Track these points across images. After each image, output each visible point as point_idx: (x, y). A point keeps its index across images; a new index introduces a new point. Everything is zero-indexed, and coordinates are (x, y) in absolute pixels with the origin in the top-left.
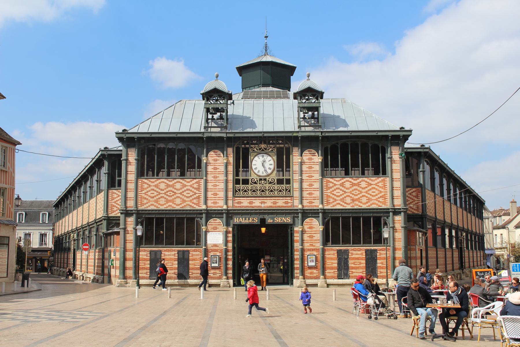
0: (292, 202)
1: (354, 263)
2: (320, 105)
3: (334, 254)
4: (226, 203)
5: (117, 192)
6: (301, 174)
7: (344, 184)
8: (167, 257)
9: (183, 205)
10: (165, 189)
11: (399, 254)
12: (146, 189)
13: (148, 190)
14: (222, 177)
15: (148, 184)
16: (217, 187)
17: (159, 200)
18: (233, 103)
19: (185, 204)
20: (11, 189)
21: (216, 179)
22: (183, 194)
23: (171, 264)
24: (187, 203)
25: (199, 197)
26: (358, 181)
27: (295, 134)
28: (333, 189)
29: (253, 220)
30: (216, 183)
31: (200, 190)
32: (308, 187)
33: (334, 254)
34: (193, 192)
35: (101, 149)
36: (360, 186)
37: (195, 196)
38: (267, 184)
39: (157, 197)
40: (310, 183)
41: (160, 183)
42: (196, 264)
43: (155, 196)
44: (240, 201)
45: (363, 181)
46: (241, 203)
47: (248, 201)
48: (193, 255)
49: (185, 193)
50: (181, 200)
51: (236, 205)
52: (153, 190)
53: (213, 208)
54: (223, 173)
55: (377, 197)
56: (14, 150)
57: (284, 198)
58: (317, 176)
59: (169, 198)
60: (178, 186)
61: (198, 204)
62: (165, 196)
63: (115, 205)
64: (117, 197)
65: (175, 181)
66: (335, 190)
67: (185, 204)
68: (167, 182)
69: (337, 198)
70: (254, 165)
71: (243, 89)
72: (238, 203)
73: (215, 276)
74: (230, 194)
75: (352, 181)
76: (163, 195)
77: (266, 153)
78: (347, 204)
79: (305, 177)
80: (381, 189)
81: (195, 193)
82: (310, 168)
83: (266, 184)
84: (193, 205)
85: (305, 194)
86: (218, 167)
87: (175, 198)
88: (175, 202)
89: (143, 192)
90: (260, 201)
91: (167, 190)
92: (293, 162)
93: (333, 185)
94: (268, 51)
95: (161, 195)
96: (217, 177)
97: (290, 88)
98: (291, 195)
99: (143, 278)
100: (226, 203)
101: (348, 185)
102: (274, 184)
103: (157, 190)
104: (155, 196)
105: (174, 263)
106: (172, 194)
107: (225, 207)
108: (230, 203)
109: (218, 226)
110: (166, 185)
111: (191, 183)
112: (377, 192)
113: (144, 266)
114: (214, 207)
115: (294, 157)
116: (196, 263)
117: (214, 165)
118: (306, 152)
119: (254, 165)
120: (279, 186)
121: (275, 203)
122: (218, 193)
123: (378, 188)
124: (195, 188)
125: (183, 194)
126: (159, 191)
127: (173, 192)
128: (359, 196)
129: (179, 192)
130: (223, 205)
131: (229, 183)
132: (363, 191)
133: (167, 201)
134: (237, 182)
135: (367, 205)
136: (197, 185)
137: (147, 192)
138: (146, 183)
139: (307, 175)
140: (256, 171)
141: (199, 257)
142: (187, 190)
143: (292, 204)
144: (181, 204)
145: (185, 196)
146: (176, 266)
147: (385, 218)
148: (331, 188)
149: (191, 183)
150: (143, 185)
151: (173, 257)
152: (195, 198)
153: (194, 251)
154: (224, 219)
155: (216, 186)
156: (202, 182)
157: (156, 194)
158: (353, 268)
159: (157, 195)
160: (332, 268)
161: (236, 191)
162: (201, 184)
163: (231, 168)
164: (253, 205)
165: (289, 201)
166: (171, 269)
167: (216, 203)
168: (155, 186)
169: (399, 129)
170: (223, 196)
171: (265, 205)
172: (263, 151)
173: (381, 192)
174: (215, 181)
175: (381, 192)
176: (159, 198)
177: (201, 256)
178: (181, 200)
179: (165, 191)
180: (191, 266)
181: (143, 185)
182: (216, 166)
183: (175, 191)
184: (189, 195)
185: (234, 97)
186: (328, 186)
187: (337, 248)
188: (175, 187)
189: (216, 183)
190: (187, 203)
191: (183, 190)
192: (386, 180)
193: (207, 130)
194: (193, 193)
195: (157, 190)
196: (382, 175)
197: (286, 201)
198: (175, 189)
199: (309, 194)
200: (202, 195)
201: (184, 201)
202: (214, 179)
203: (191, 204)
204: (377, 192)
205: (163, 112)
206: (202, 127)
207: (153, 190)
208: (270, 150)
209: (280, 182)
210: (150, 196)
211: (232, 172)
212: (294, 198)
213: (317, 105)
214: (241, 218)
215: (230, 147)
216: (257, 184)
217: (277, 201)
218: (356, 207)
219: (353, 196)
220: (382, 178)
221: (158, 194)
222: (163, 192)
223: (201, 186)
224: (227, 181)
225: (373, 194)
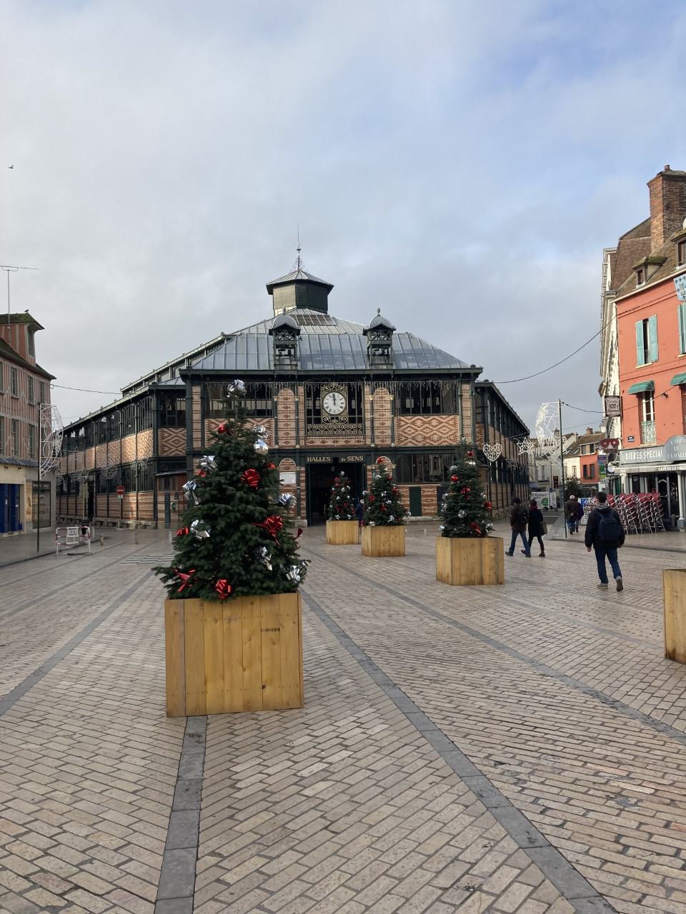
1: (426, 501)
5: (168, 431)
14: (293, 416)
16: (289, 427)
26: (429, 419)
27: (367, 373)
28: (404, 427)
29: (326, 459)
45: (434, 419)
51: (309, 444)
55: (448, 435)
58: (389, 415)
66: (407, 428)
69: (409, 437)
74: (302, 433)
75: (423, 419)
78: (419, 442)
80: (451, 427)
85: (377, 433)
92: (364, 401)
96: (287, 416)
97: (327, 309)
100: (298, 442)
101: (419, 423)
107: (298, 447)
108: (302, 443)
112: (448, 430)
121: (346, 442)
123: (449, 426)
128: (430, 434)
132: (434, 429)
134: (309, 421)
135: (438, 442)
140: (328, 410)
148: (402, 426)
155: (288, 425)
158: (425, 505)
165: (362, 440)
169: (469, 367)
172: (334, 390)
173: (452, 430)
175: (452, 430)
187: (410, 486)
204: (448, 430)
206: (272, 364)
209: (352, 421)
213: (388, 342)
218: (427, 445)
219: (424, 434)
224: (297, 421)
225: (444, 432)
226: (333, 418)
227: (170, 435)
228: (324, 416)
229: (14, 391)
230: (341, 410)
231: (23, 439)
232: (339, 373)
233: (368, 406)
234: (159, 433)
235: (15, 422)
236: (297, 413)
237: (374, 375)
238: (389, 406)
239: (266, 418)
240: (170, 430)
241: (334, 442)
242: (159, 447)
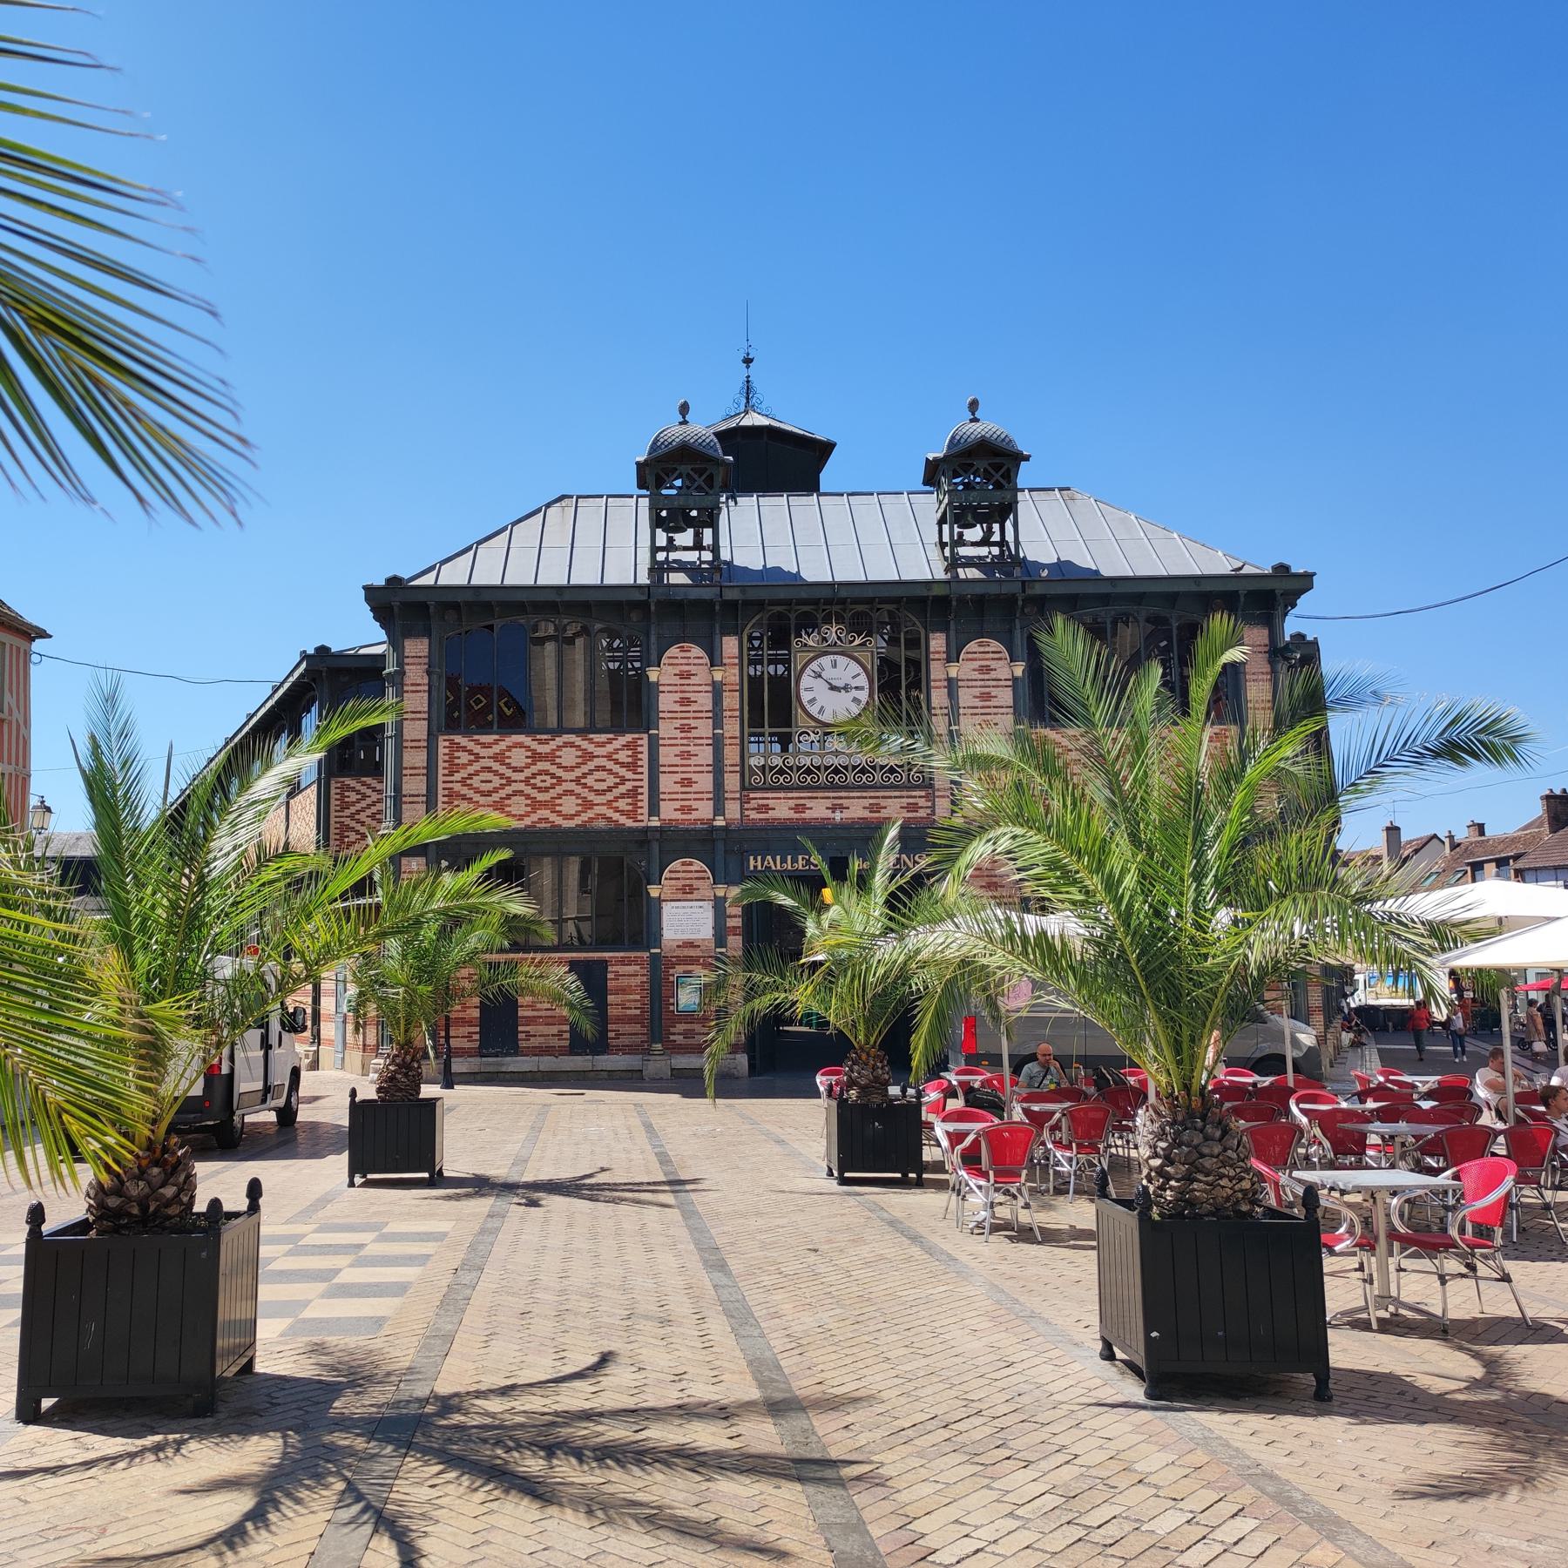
0: (930, 804)
5: (358, 786)
9: (585, 817)
10: (527, 766)
12: (464, 766)
13: (471, 769)
14: (704, 729)
15: (470, 752)
16: (693, 761)
17: (507, 802)
19: (590, 814)
20: (17, 776)
21: (689, 735)
22: (583, 781)
24: (598, 810)
25: (633, 793)
27: (937, 591)
31: (640, 770)
34: (616, 775)
35: (305, 652)
37: (622, 789)
39: (503, 793)
41: (509, 748)
42: (628, 1005)
43: (496, 790)
44: (765, 802)
46: (767, 808)
47: (792, 803)
48: (618, 976)
49: (589, 781)
50: (580, 801)
51: (754, 815)
52: (489, 769)
56: (27, 654)
57: (905, 793)
59: (541, 797)
60: (569, 757)
61: (632, 814)
62: (528, 790)
63: (353, 824)
64: (358, 801)
67: (590, 814)
68: (534, 745)
70: (806, 690)
72: (760, 809)
73: (690, 1041)
74: (732, 782)
76: (521, 786)
81: (623, 780)
84: (616, 816)
86: (693, 697)
87: (559, 796)
88: (558, 808)
89: (457, 777)
90: (829, 803)
91: (534, 769)
95: (515, 787)
99: (463, 1053)
103: (503, 769)
104: (496, 790)
106: (550, 781)
107: (720, 822)
108: (733, 810)
109: (696, 883)
110: (529, 754)
111: (610, 748)
113: (461, 1015)
115: (933, 665)
116: (629, 1001)
117: (682, 692)
118: (972, 646)
119: (806, 690)
122: (694, 777)
124: (622, 765)
125: (583, 781)
126: (509, 773)
127: (553, 776)
129: (572, 775)
131: (727, 750)
133: (535, 805)
137: (470, 776)
138: (464, 749)
140: (814, 710)
141: (639, 980)
142: (598, 768)
143: (929, 811)
144: (578, 814)
145: (591, 789)
149: (610, 748)
150: (456, 754)
152: (623, 796)
153: (623, 962)
155: (689, 755)
156: (645, 742)
157: (497, 782)
159: (502, 786)
161: (752, 773)
162: (639, 749)
163: (731, 701)
164: (808, 815)
165: (922, 802)
167: (690, 810)
168: (495, 758)
171: (844, 816)
174: (685, 742)
176: (509, 797)
178: (580, 801)
179: (528, 773)
180: (612, 1012)
181: (456, 754)
182: (687, 695)
183: (560, 773)
184: (603, 786)
188: (558, 760)
190: (598, 810)
191: (585, 769)
194: (618, 780)
195: (503, 769)
197: (911, 801)
198: (560, 766)
200: (645, 783)
201: (588, 805)
202: (683, 735)
203: (610, 813)
205: (508, 532)
207: (489, 769)
208: (856, 642)
210: (477, 791)
211: (737, 713)
212: (937, 794)
214: (769, 857)
215: (728, 634)
217: (883, 802)
221: (504, 781)
222: (521, 776)
223: (640, 756)
227: (364, 797)
230: (855, 710)
233: (939, 697)
234: (333, 791)
236: (717, 718)
238: (1005, 697)
240: (364, 784)
241: (833, 809)
242: (332, 831)
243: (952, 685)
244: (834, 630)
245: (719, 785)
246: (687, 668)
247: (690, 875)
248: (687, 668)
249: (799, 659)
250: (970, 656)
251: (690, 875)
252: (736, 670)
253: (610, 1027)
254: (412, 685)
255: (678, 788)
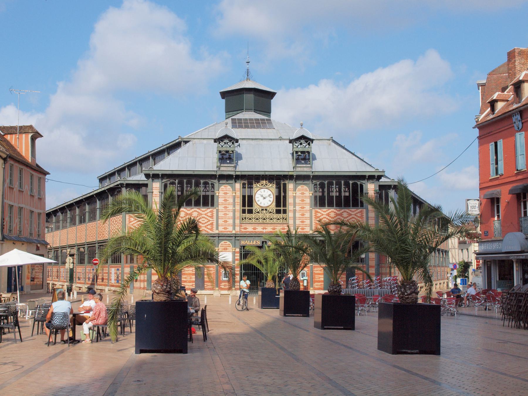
2: (311, 150)
3: (321, 271)
4: (234, 229)
6: (295, 206)
7: (330, 214)
8: (187, 272)
11: (373, 270)
14: (231, 207)
16: (228, 216)
18: (239, 145)
23: (190, 278)
25: (212, 224)
26: (341, 212)
27: (290, 173)
30: (226, 213)
31: (213, 218)
32: (301, 216)
33: (321, 271)
36: (343, 216)
37: (209, 223)
38: (268, 214)
40: (302, 213)
45: (345, 211)
47: (253, 227)
51: (243, 230)
53: (224, 233)
54: (232, 204)
57: (281, 225)
58: (308, 207)
61: (211, 229)
65: (193, 210)
68: (186, 211)
70: (257, 198)
71: (226, 112)
74: (237, 222)
77: (266, 188)
79: (298, 208)
81: (209, 221)
82: (303, 200)
83: (267, 213)
84: (207, 230)
86: (228, 199)
90: (262, 227)
92: (288, 196)
93: (321, 215)
94: (250, 76)
97: (270, 113)
98: (287, 223)
100: (234, 229)
102: (274, 213)
105: (192, 277)
107: (234, 232)
108: (237, 229)
109: (228, 248)
110: (185, 213)
111: (206, 212)
114: (225, 232)
115: (290, 192)
118: (300, 187)
119: (257, 198)
120: (277, 215)
121: (274, 229)
122: (228, 220)
124: (209, 216)
130: (232, 230)
131: (236, 213)
134: (244, 212)
136: (211, 213)
139: (300, 206)
140: (259, 203)
142: (203, 217)
146: (194, 279)
147: (362, 242)
149: (206, 212)
151: (191, 272)
152: (209, 225)
154: (233, 241)
155: (227, 214)
156: (215, 210)
160: (319, 282)
162: (214, 213)
164: (257, 230)
166: (190, 282)
167: (226, 228)
170: (232, 223)
172: (264, 186)
177: (214, 272)
184: (204, 222)
185: (240, 142)
186: (317, 216)
189: (226, 213)
192: (363, 211)
193: (219, 169)
194: (208, 221)
196: (360, 207)
197: (283, 227)
199: (302, 222)
200: (215, 221)
202: (225, 209)
203: (206, 229)
209: (278, 212)
211: (239, 204)
214: (246, 241)
216: (259, 213)
217: (276, 227)
220: (360, 210)
223: (214, 214)
226: (262, 210)
228: (255, 207)
229: (20, 186)
230: (270, 203)
231: (26, 222)
232: (267, 173)
235: (21, 209)
237: (297, 176)
238: (308, 201)
239: (209, 208)
241: (263, 229)
243: (295, 198)
244: (264, 182)
245: (234, 222)
246: (226, 192)
247: (226, 245)
248: (226, 192)
249: (255, 190)
250: (299, 190)
251: (226, 245)
252: (239, 192)
253: (205, 283)
254: (155, 195)
255: (223, 223)
